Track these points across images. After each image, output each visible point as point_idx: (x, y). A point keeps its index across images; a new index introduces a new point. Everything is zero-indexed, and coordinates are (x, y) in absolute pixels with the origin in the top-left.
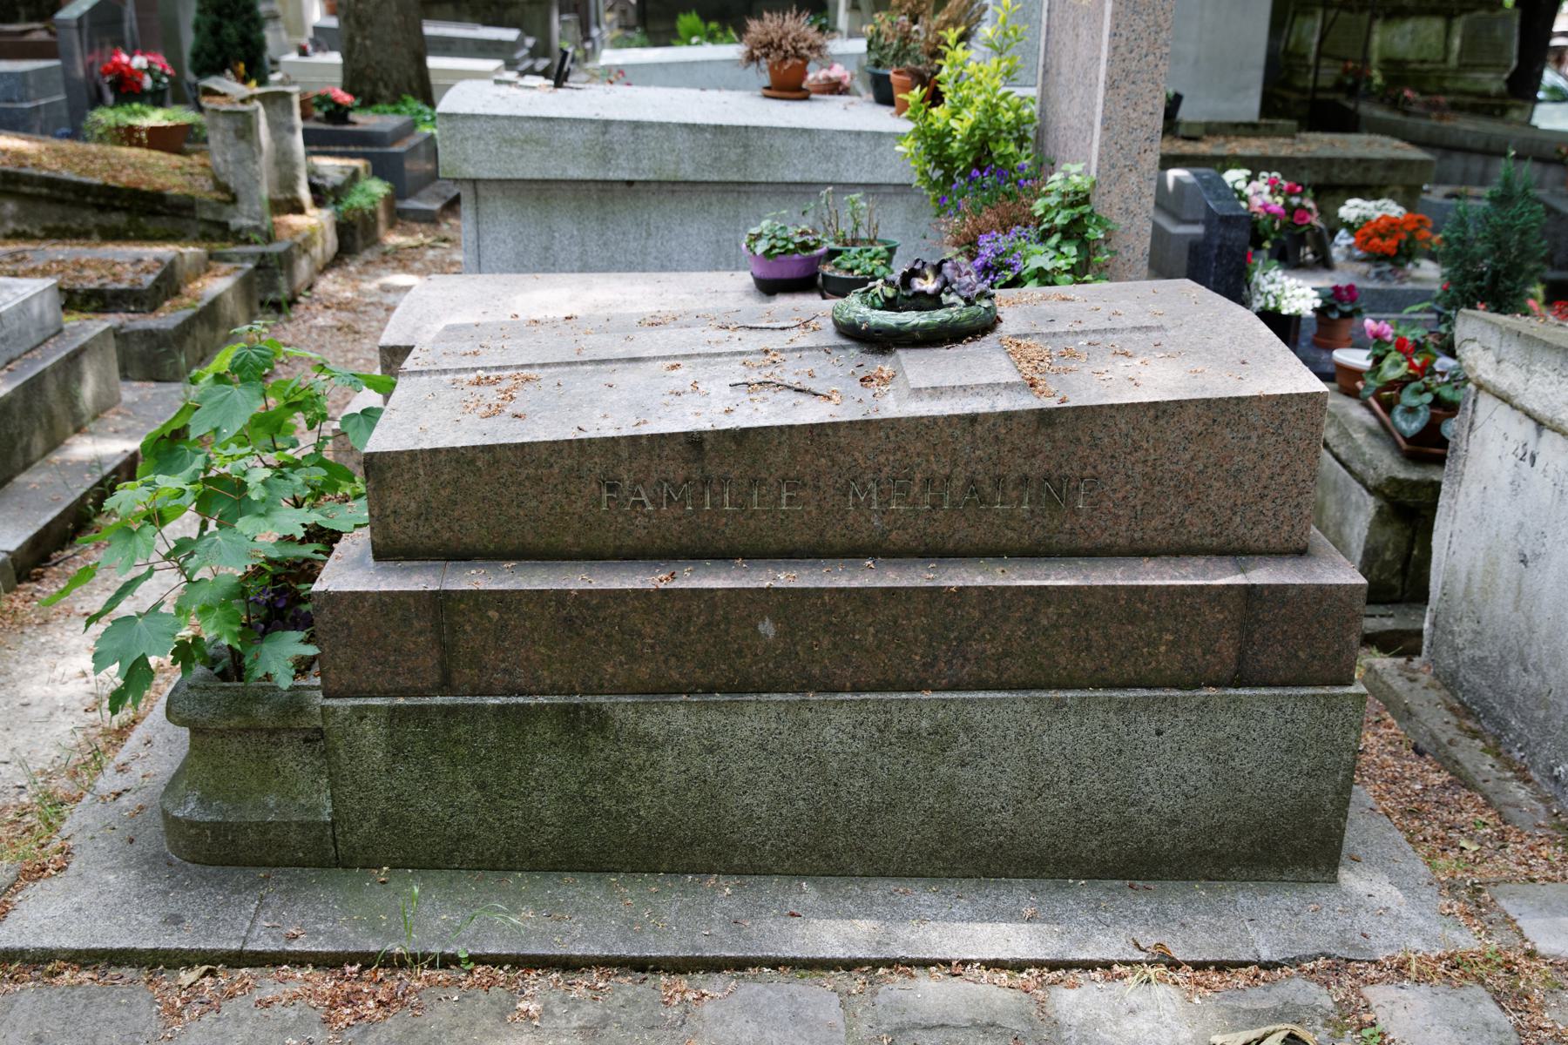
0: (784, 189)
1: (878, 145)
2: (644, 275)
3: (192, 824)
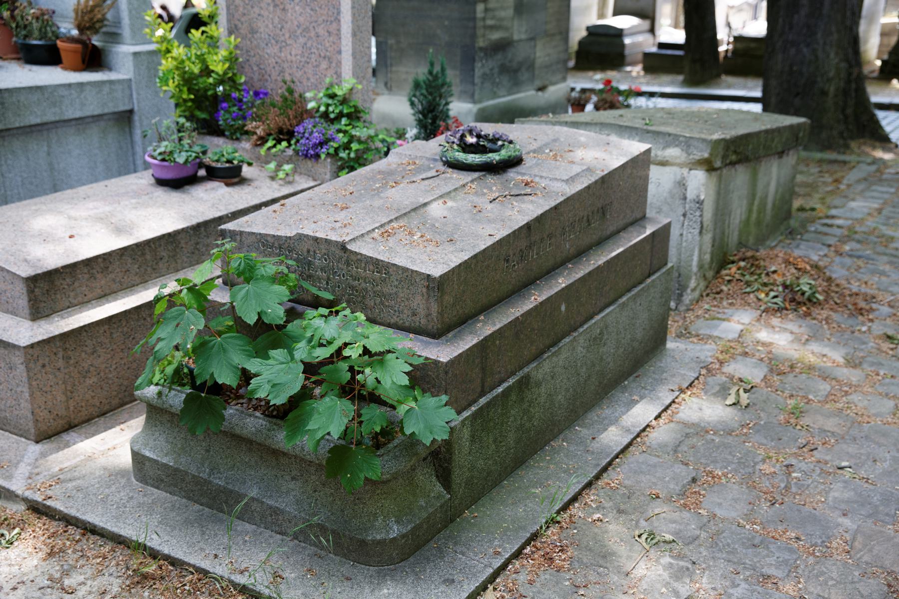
0: (28, 130)
1: (82, 91)
2: (8, 206)
3: (403, 536)
